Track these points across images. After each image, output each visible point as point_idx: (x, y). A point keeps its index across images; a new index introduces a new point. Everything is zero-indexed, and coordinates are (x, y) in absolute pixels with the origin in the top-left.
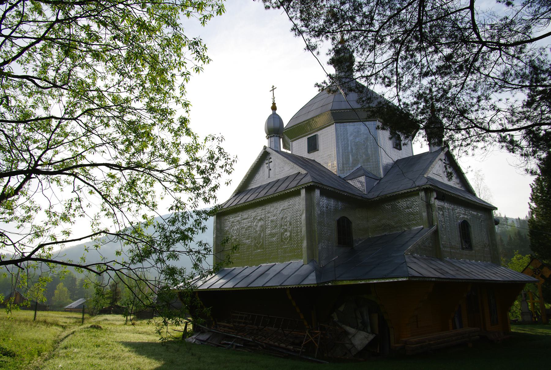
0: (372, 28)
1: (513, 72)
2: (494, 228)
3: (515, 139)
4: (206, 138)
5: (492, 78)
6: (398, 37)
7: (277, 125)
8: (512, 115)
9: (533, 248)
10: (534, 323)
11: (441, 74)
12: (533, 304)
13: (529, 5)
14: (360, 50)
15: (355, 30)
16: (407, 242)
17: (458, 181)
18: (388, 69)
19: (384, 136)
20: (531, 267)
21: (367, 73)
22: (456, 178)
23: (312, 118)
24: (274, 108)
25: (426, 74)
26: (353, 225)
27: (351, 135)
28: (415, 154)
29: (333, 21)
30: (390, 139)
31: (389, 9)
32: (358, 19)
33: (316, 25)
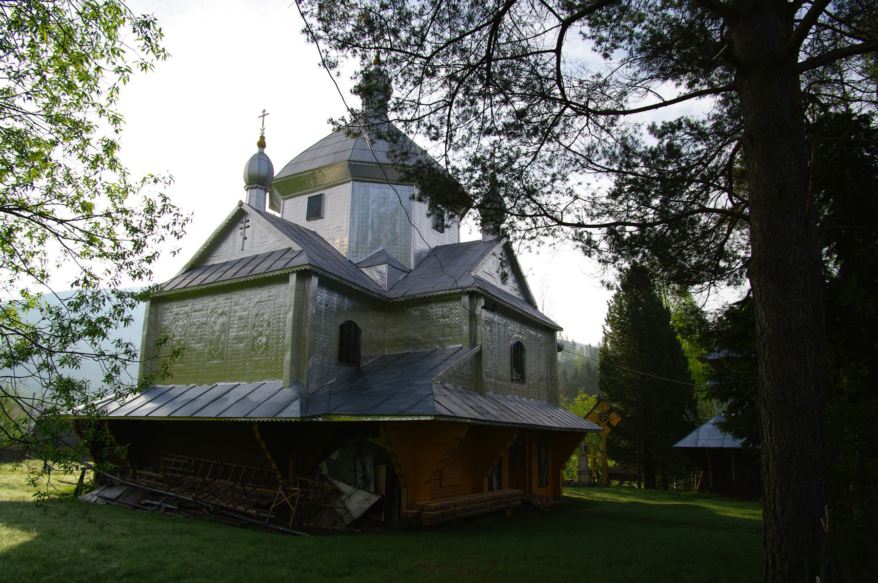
0: (421, 52)
1: (600, 149)
2: (556, 355)
3: (594, 238)
4: (144, 179)
5: (575, 153)
6: (457, 72)
7: (264, 172)
8: (593, 206)
9: (603, 386)
10: (592, 485)
11: (508, 135)
12: (594, 460)
13: (628, 64)
14: (401, 80)
15: (396, 50)
16: (438, 365)
17: (516, 286)
18: (437, 115)
19: (420, 210)
20: (597, 412)
21: (406, 116)
22: (514, 282)
23: (319, 169)
24: (262, 144)
25: (488, 132)
26: (363, 335)
27: (374, 201)
28: (461, 241)
29: (366, 30)
30: (429, 215)
31: (448, 30)
32: (403, 35)
33: (341, 31)
